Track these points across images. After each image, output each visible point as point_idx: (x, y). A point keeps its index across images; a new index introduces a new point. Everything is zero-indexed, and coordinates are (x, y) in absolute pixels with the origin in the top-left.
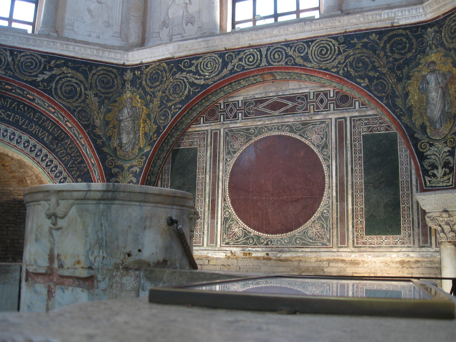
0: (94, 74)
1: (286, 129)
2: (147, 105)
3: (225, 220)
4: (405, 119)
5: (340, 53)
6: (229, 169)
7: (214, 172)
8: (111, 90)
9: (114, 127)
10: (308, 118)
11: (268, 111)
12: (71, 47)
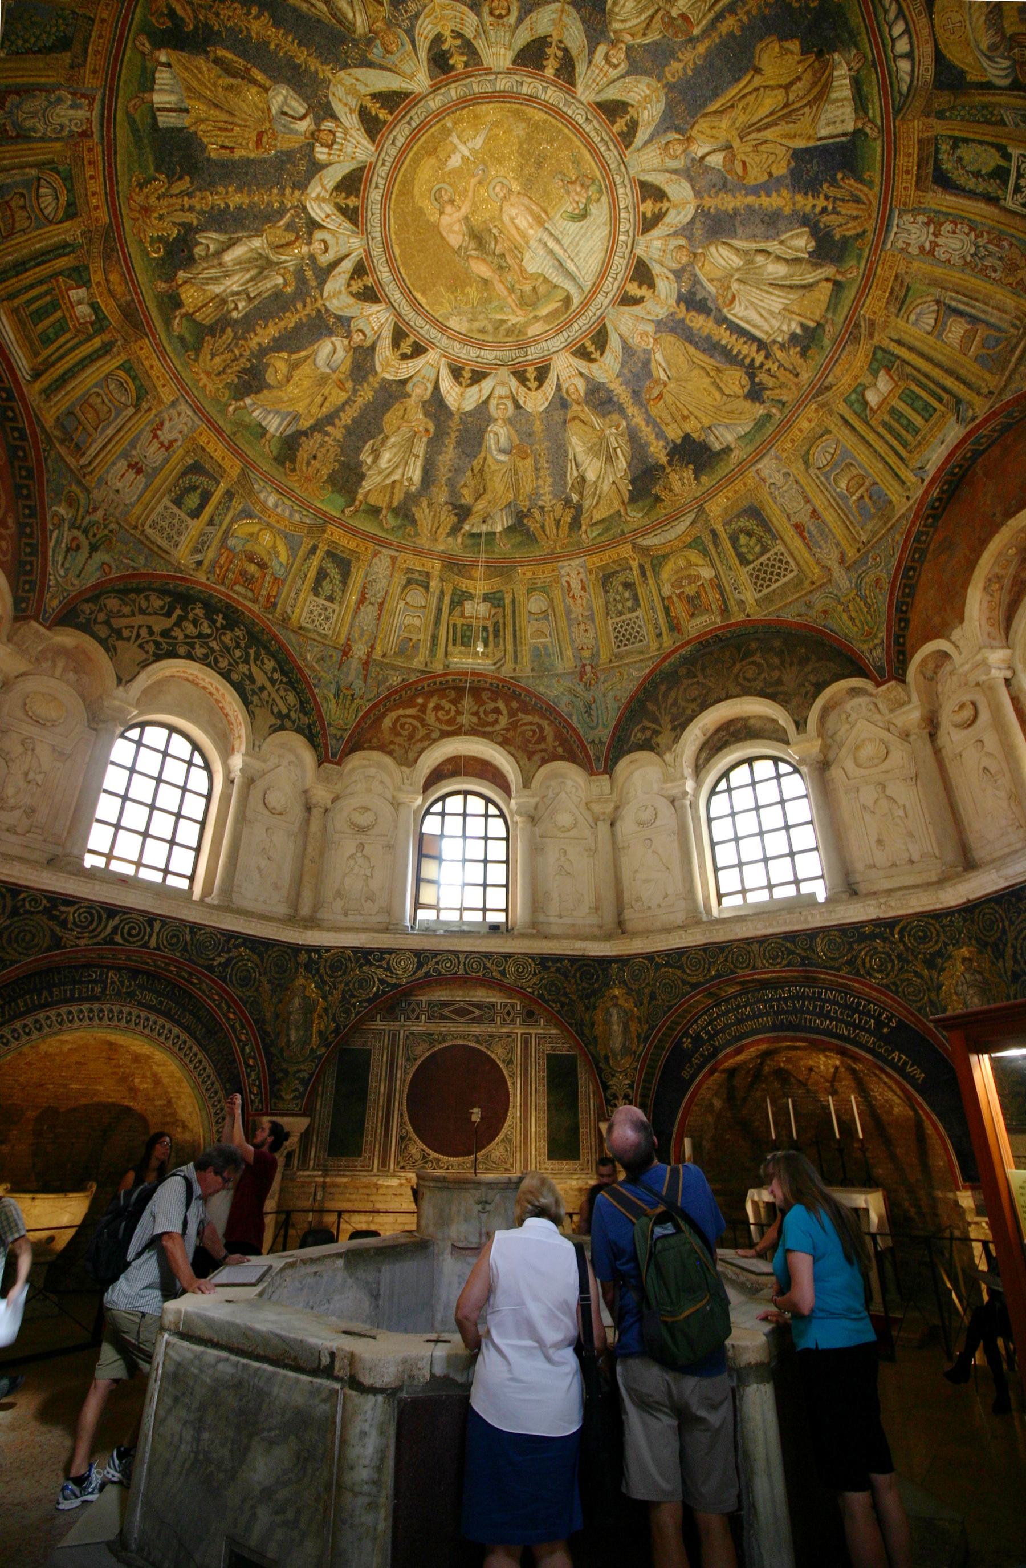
2: (324, 998)
4: (591, 1047)
5: (535, 974)
6: (409, 1077)
7: (391, 1081)
11: (453, 1016)
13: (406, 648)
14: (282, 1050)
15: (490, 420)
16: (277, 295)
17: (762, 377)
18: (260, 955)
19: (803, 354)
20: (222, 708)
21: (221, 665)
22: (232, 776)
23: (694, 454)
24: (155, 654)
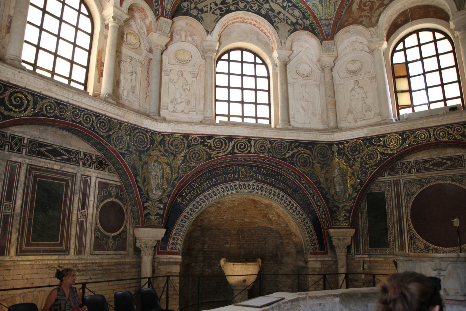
0: (316, 149)
1: (449, 179)
2: (351, 167)
3: (411, 238)
6: (410, 205)
7: (399, 208)
8: (326, 159)
9: (331, 182)
10: (464, 172)
12: (302, 134)
14: (333, 196)
18: (311, 150)
20: (262, 31)
21: (254, 8)
22: (276, 62)
24: (221, 14)
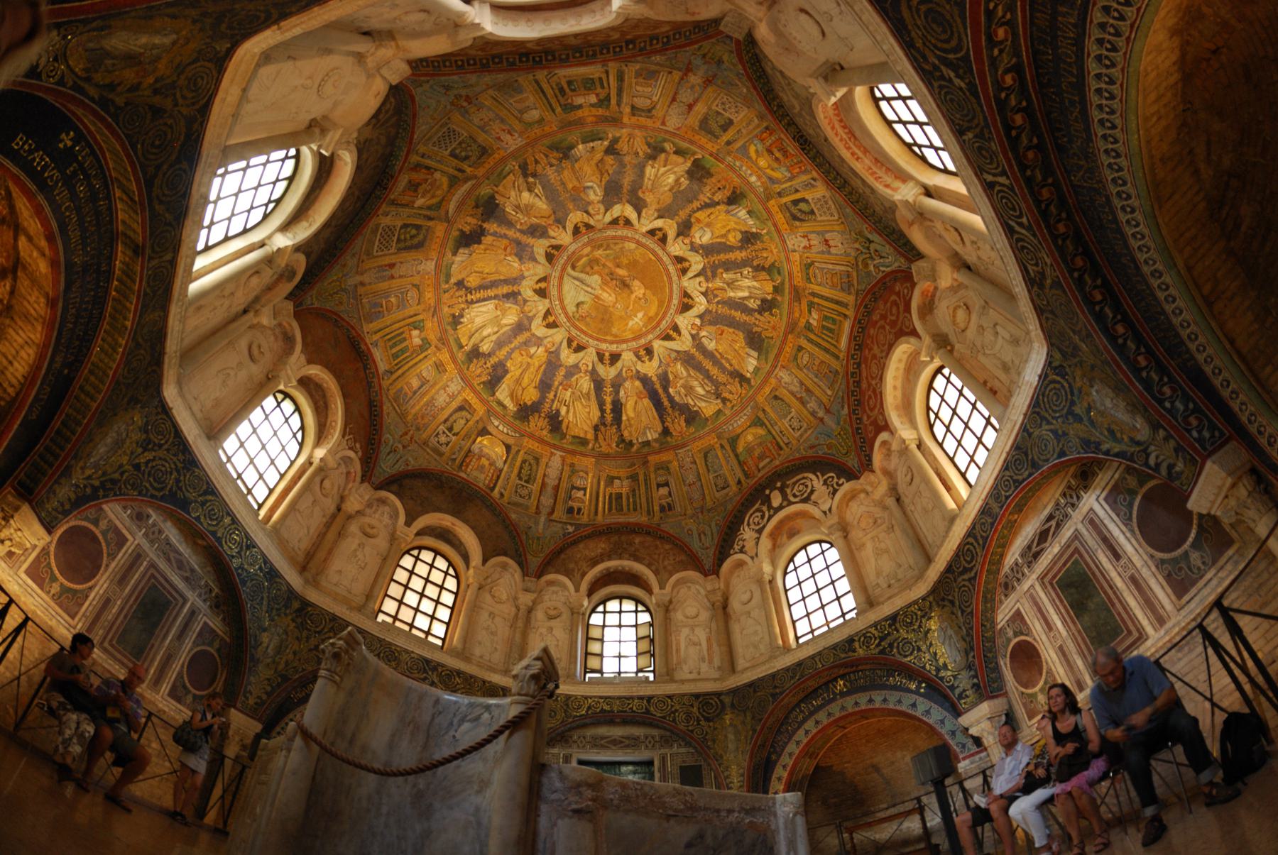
13: (650, 76)
15: (603, 202)
16: (727, 270)
17: (462, 292)
19: (454, 316)
23: (470, 239)
